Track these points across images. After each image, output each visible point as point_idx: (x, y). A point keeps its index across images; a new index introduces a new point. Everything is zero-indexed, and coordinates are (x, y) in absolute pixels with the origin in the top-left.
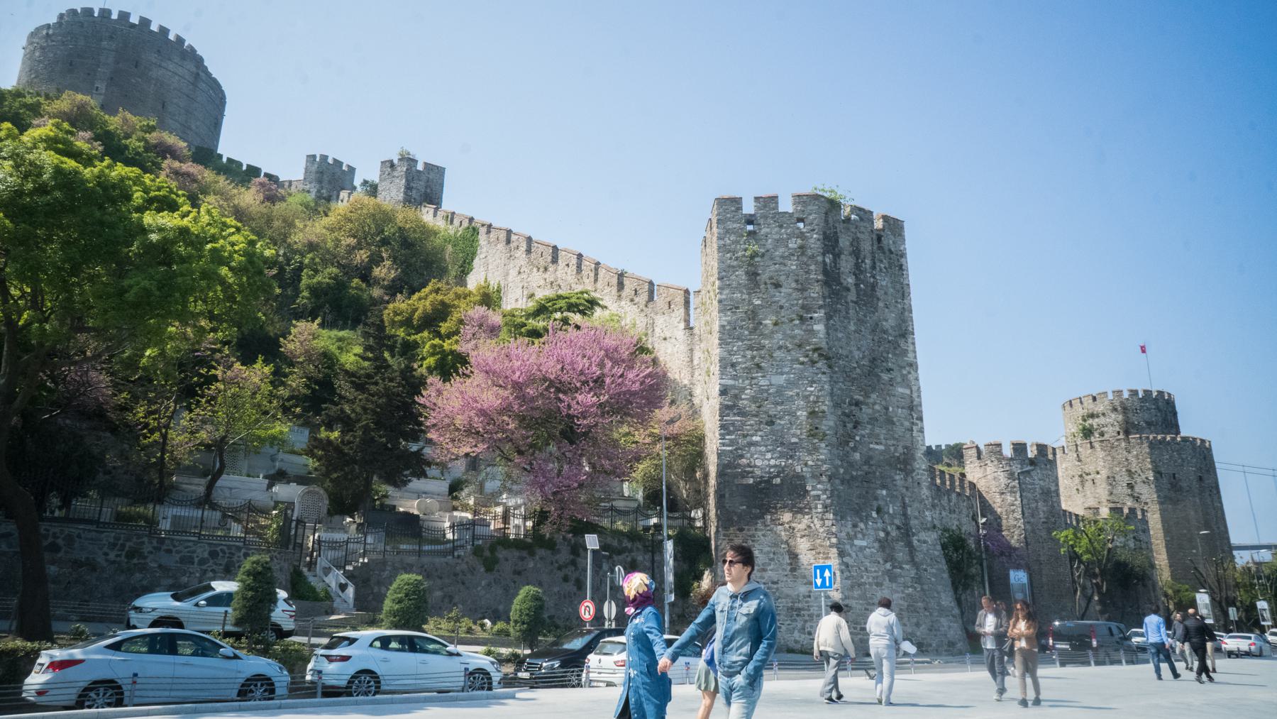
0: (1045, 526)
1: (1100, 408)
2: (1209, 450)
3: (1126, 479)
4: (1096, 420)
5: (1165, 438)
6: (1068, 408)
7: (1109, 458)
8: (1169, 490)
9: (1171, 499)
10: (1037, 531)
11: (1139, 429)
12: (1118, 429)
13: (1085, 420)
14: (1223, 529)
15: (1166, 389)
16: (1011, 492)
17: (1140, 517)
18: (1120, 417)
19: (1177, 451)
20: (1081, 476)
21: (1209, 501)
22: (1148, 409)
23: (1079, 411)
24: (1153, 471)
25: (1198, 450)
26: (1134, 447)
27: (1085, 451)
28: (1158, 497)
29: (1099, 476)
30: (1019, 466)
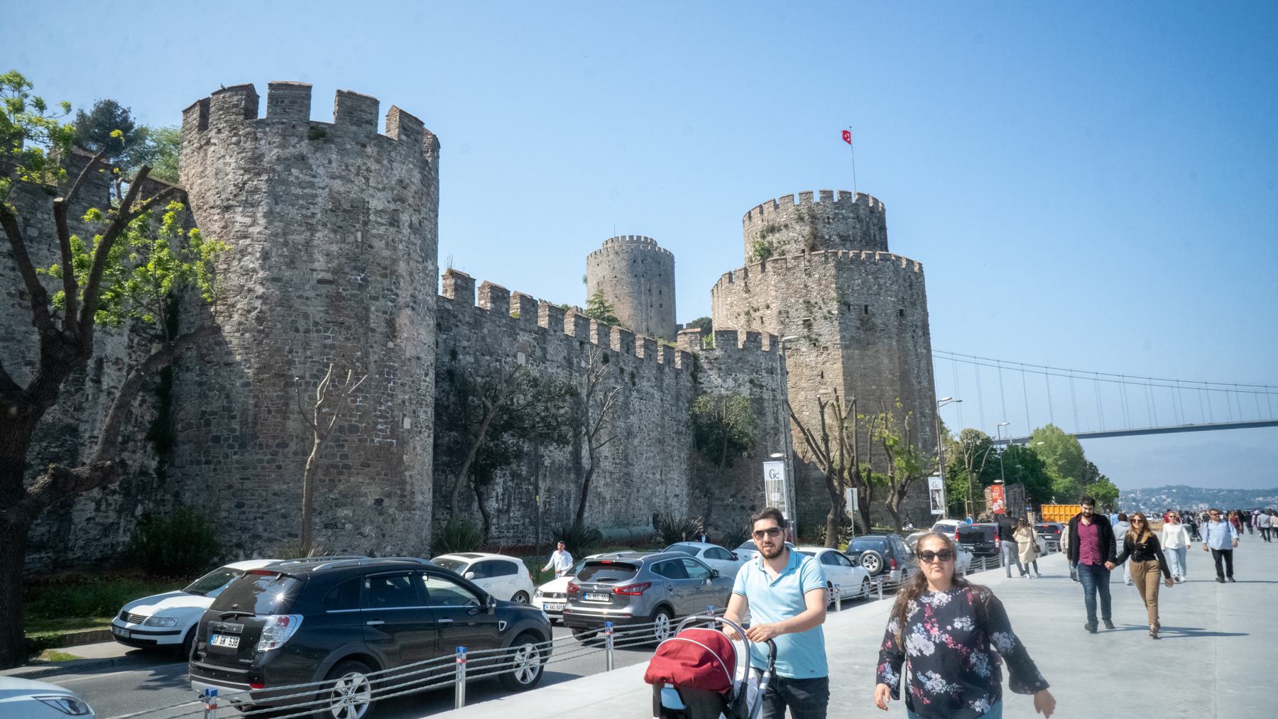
0: (324, 289)
1: (783, 219)
2: (920, 274)
3: (803, 314)
4: (777, 235)
5: (858, 256)
6: (747, 222)
7: (783, 285)
8: (858, 328)
9: (858, 341)
10: (297, 303)
11: (827, 243)
12: (802, 246)
13: (763, 237)
14: (925, 384)
15: (872, 192)
16: (246, 204)
17: (766, 348)
18: (807, 230)
19: (873, 274)
20: (748, 313)
21: (910, 345)
22: (845, 218)
23: (758, 224)
24: (839, 302)
25: (903, 273)
26: (817, 267)
27: (756, 275)
28: (842, 338)
29: (769, 312)
30: (277, 140)
